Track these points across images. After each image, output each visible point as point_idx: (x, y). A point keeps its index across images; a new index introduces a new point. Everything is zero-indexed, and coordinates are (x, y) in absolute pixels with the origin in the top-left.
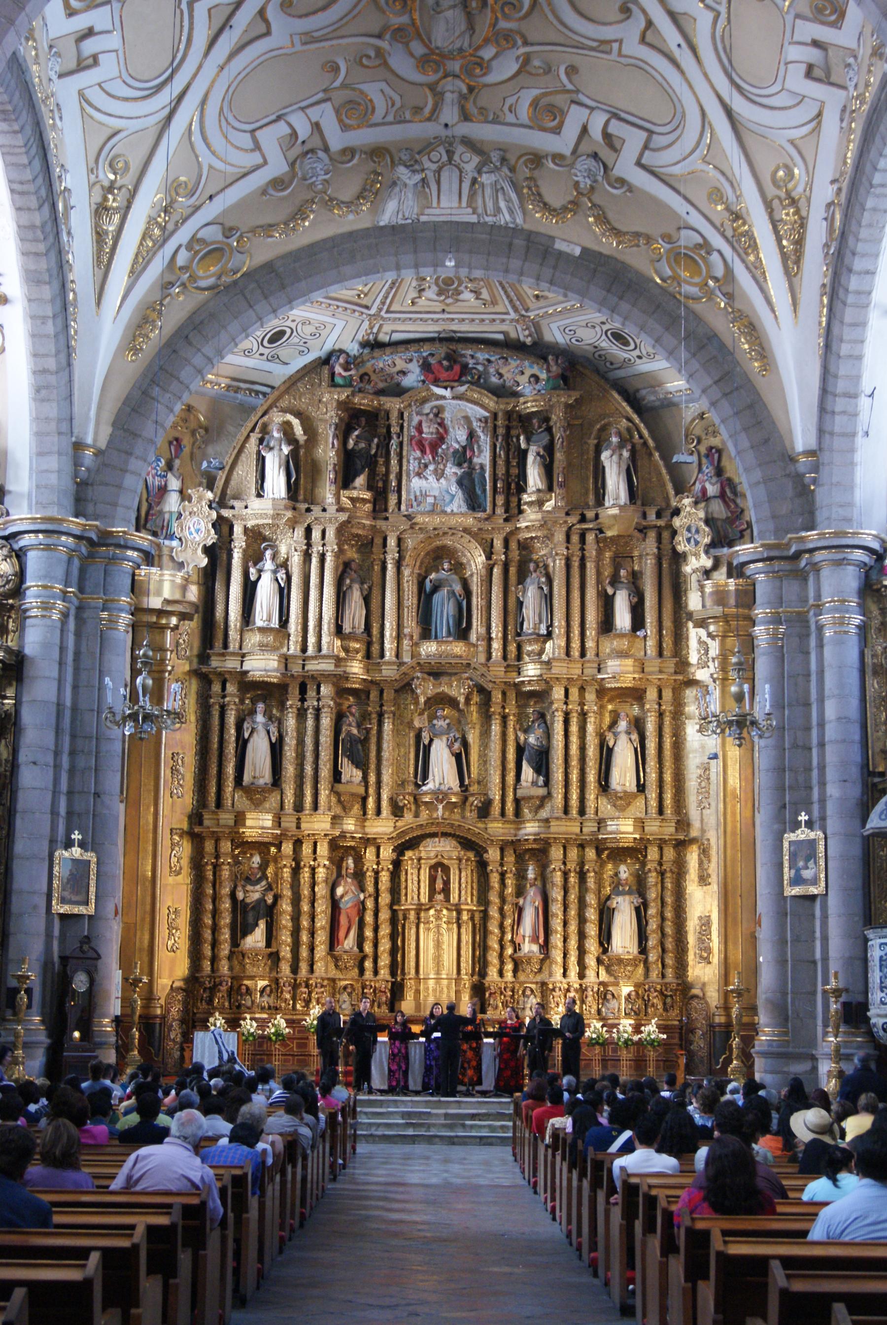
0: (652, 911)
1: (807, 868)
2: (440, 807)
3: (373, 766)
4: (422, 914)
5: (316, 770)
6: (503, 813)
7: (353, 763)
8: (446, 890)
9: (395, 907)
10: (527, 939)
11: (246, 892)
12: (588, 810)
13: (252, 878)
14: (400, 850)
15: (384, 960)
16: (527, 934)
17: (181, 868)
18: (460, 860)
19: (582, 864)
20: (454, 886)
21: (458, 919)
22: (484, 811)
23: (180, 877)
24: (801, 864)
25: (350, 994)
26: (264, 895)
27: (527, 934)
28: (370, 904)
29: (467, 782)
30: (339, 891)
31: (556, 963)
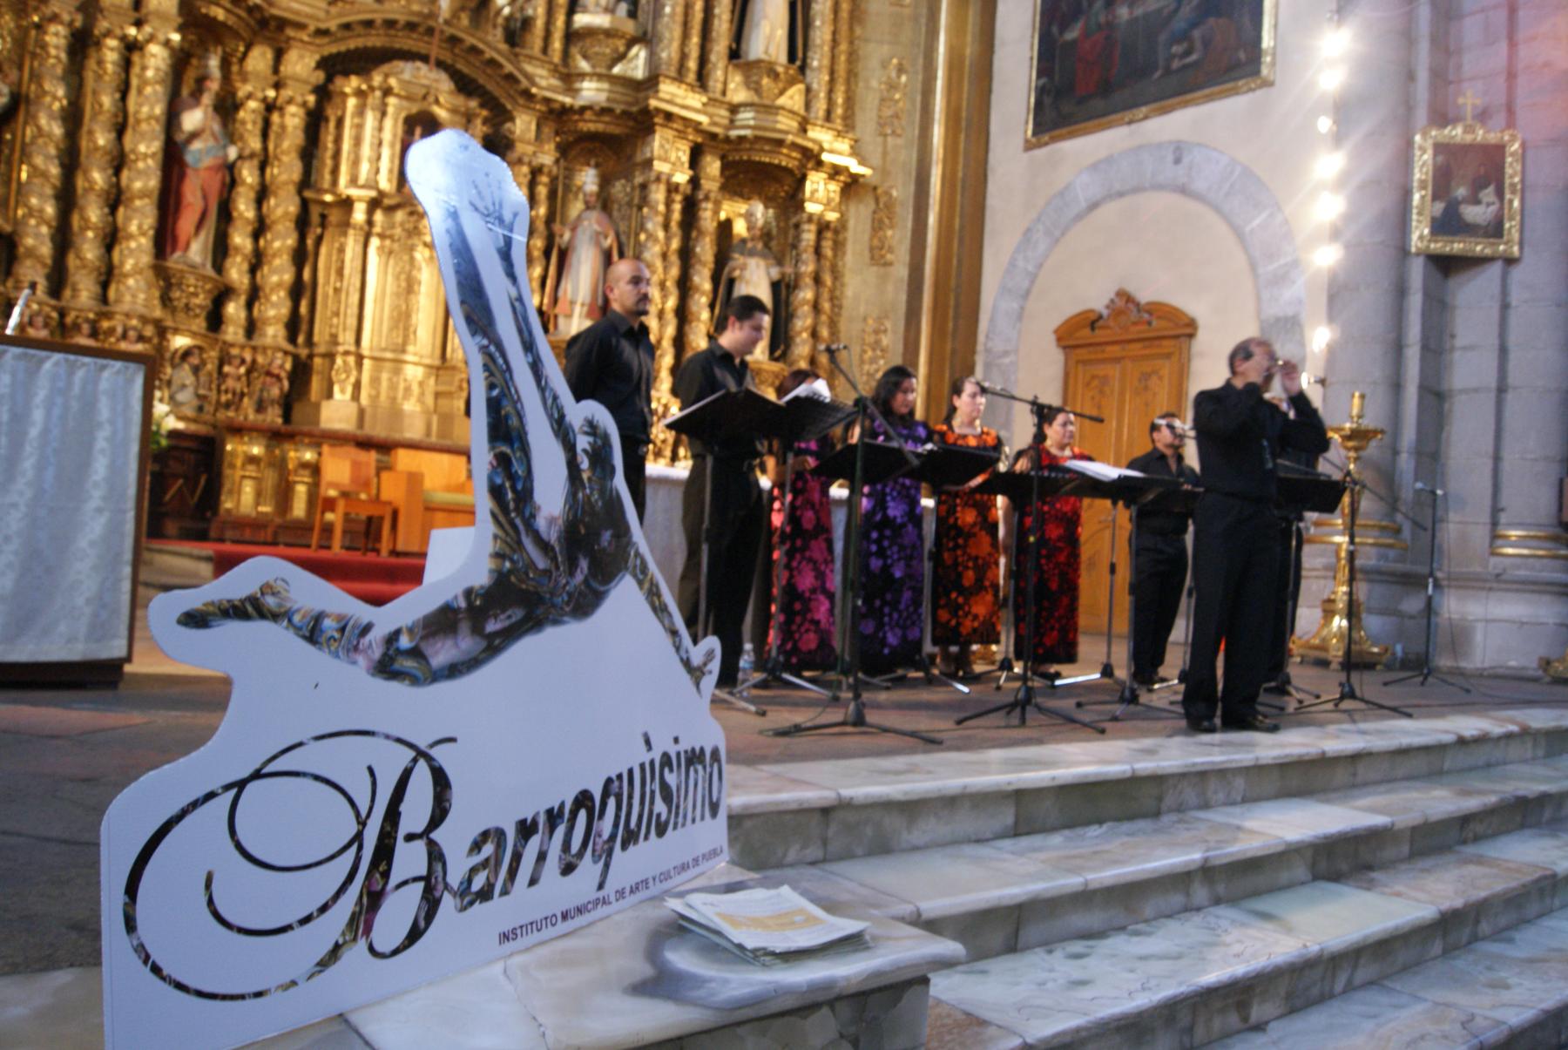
0: (806, 294)
1: (1476, 201)
4: (379, 216)
6: (545, 50)
9: (308, 194)
10: (578, 310)
12: (711, 83)
14: (334, 66)
15: (275, 308)
16: (580, 301)
19: (695, 182)
22: (516, 32)
24: (1461, 192)
25: (196, 370)
27: (580, 301)
30: (192, 119)
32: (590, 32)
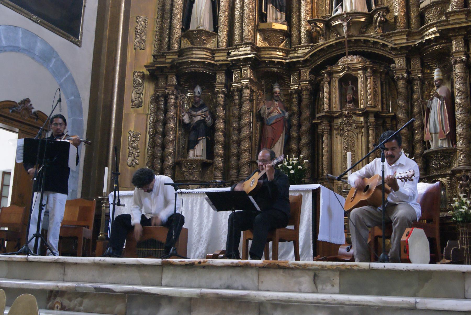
2: (345, 24)
3: (294, 10)
5: (242, 14)
7: (276, 7)
8: (355, 101)
11: (191, 117)
13: (197, 106)
14: (316, 72)
17: (141, 102)
18: (364, 69)
20: (361, 93)
21: (366, 122)
23: (140, 108)
26: (205, 118)
28: (295, 122)
29: (374, 7)
31: (463, 152)
32: (426, 8)
